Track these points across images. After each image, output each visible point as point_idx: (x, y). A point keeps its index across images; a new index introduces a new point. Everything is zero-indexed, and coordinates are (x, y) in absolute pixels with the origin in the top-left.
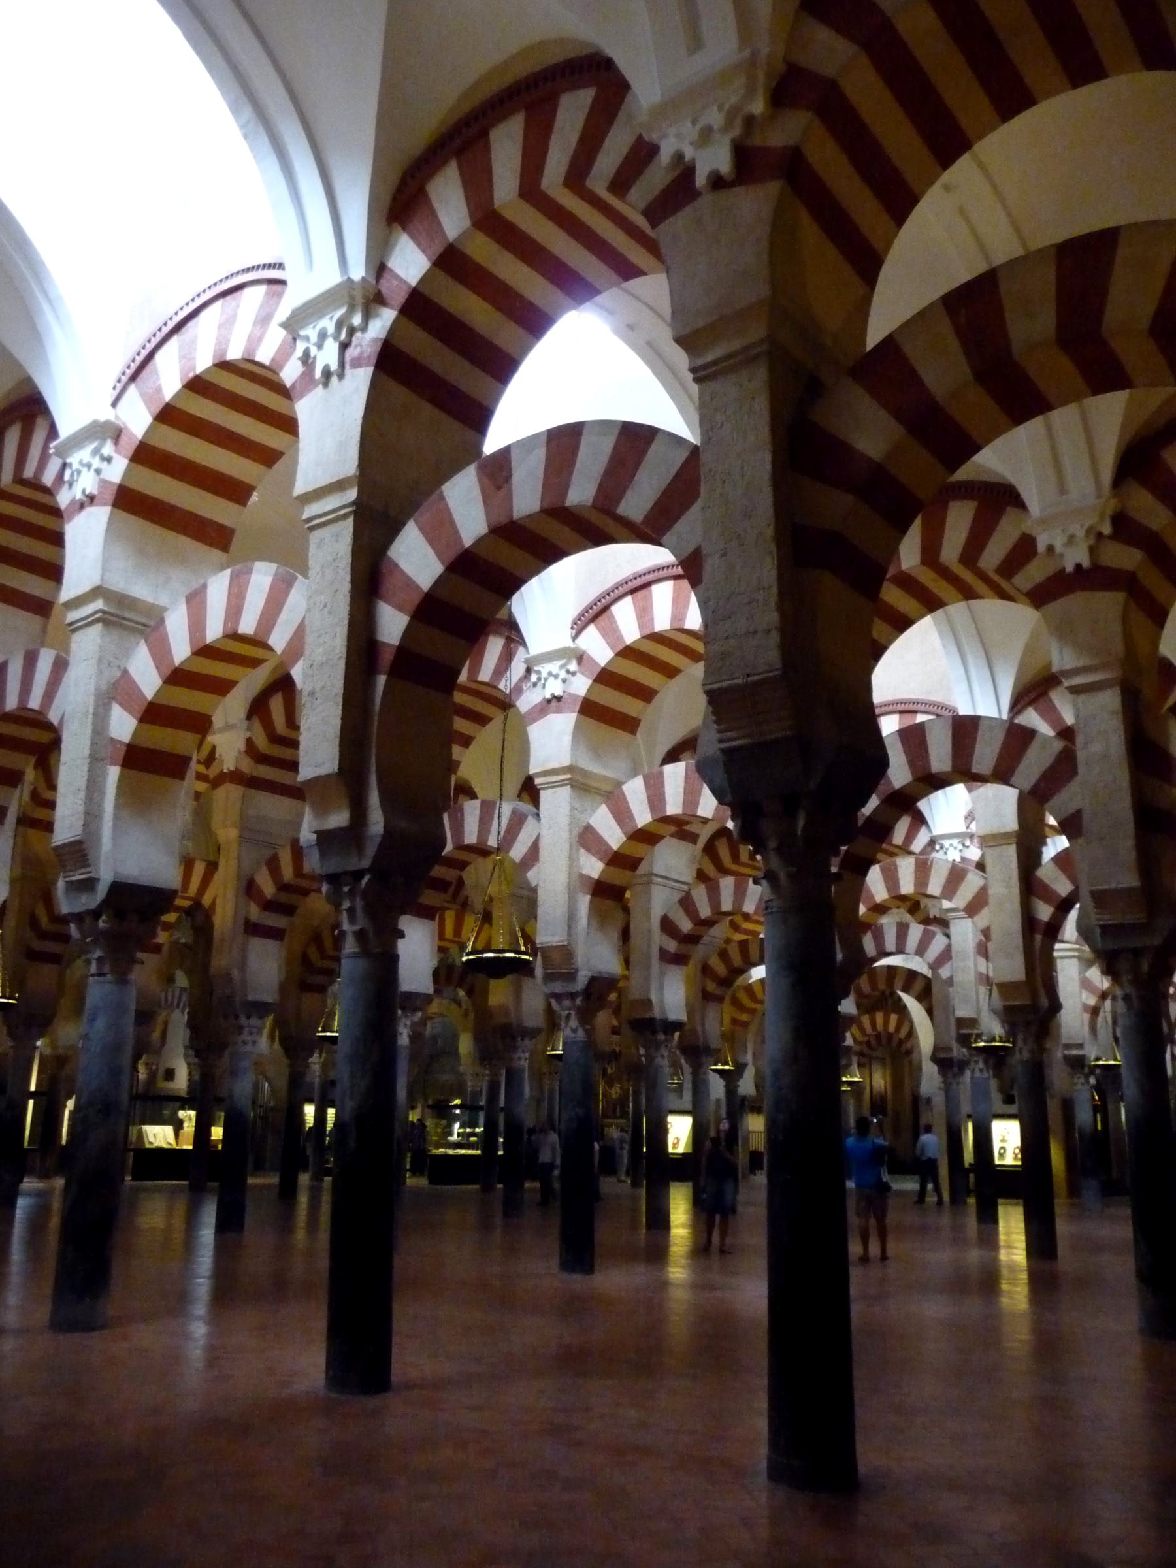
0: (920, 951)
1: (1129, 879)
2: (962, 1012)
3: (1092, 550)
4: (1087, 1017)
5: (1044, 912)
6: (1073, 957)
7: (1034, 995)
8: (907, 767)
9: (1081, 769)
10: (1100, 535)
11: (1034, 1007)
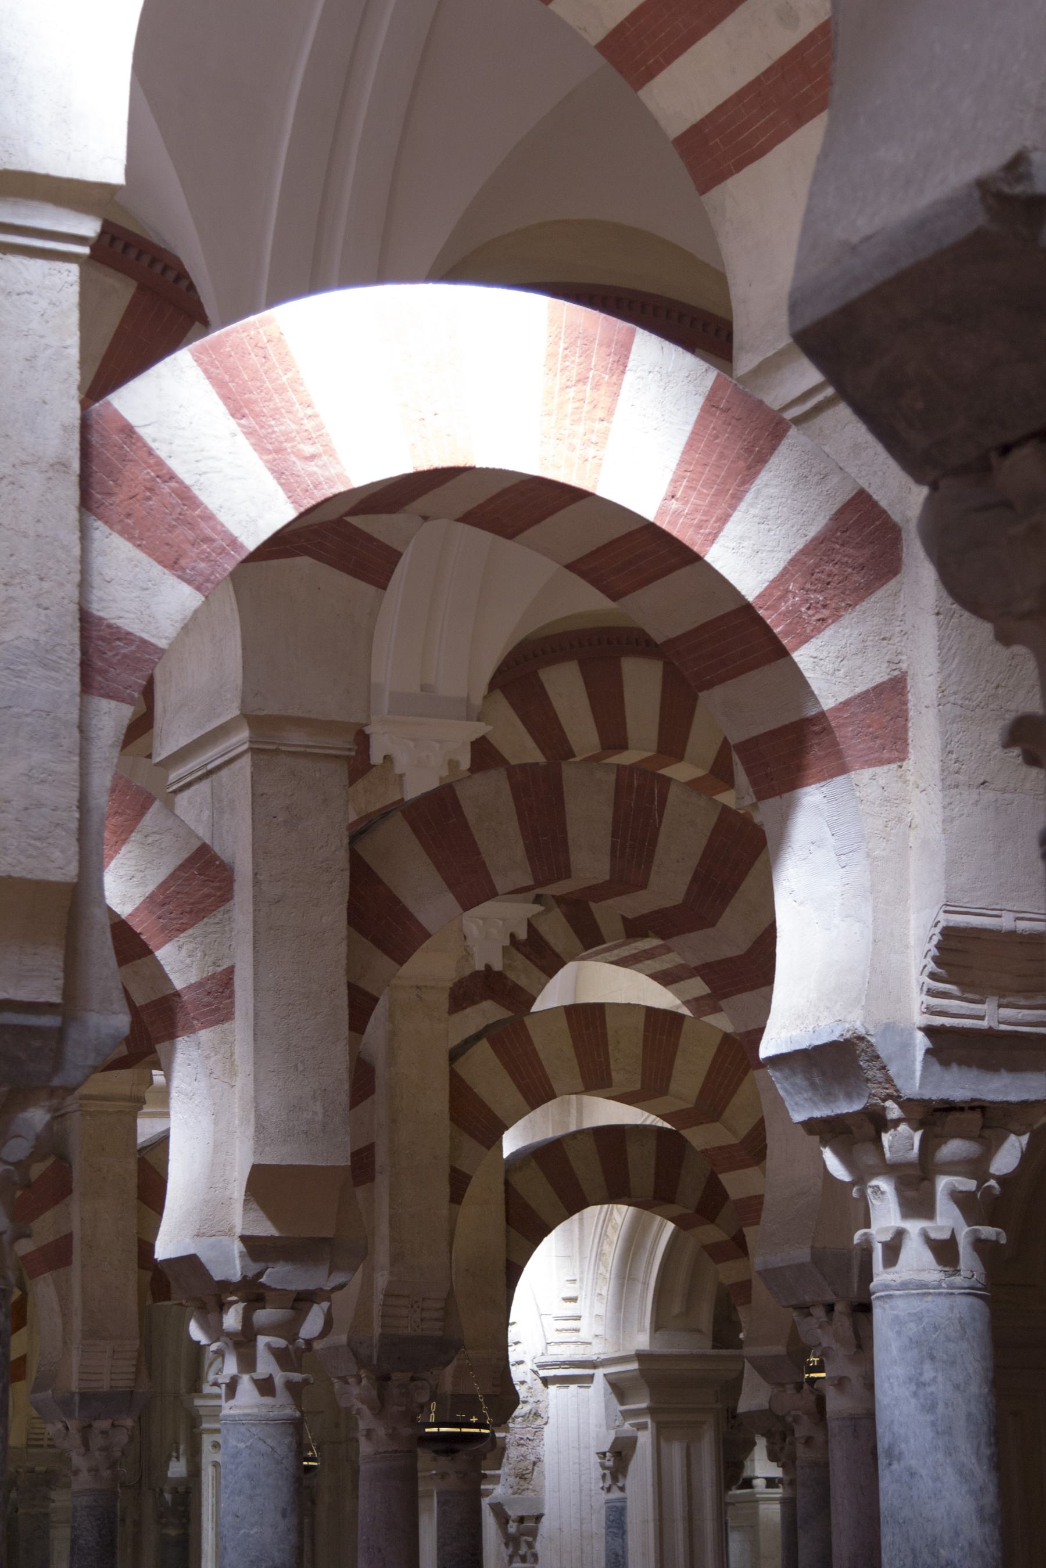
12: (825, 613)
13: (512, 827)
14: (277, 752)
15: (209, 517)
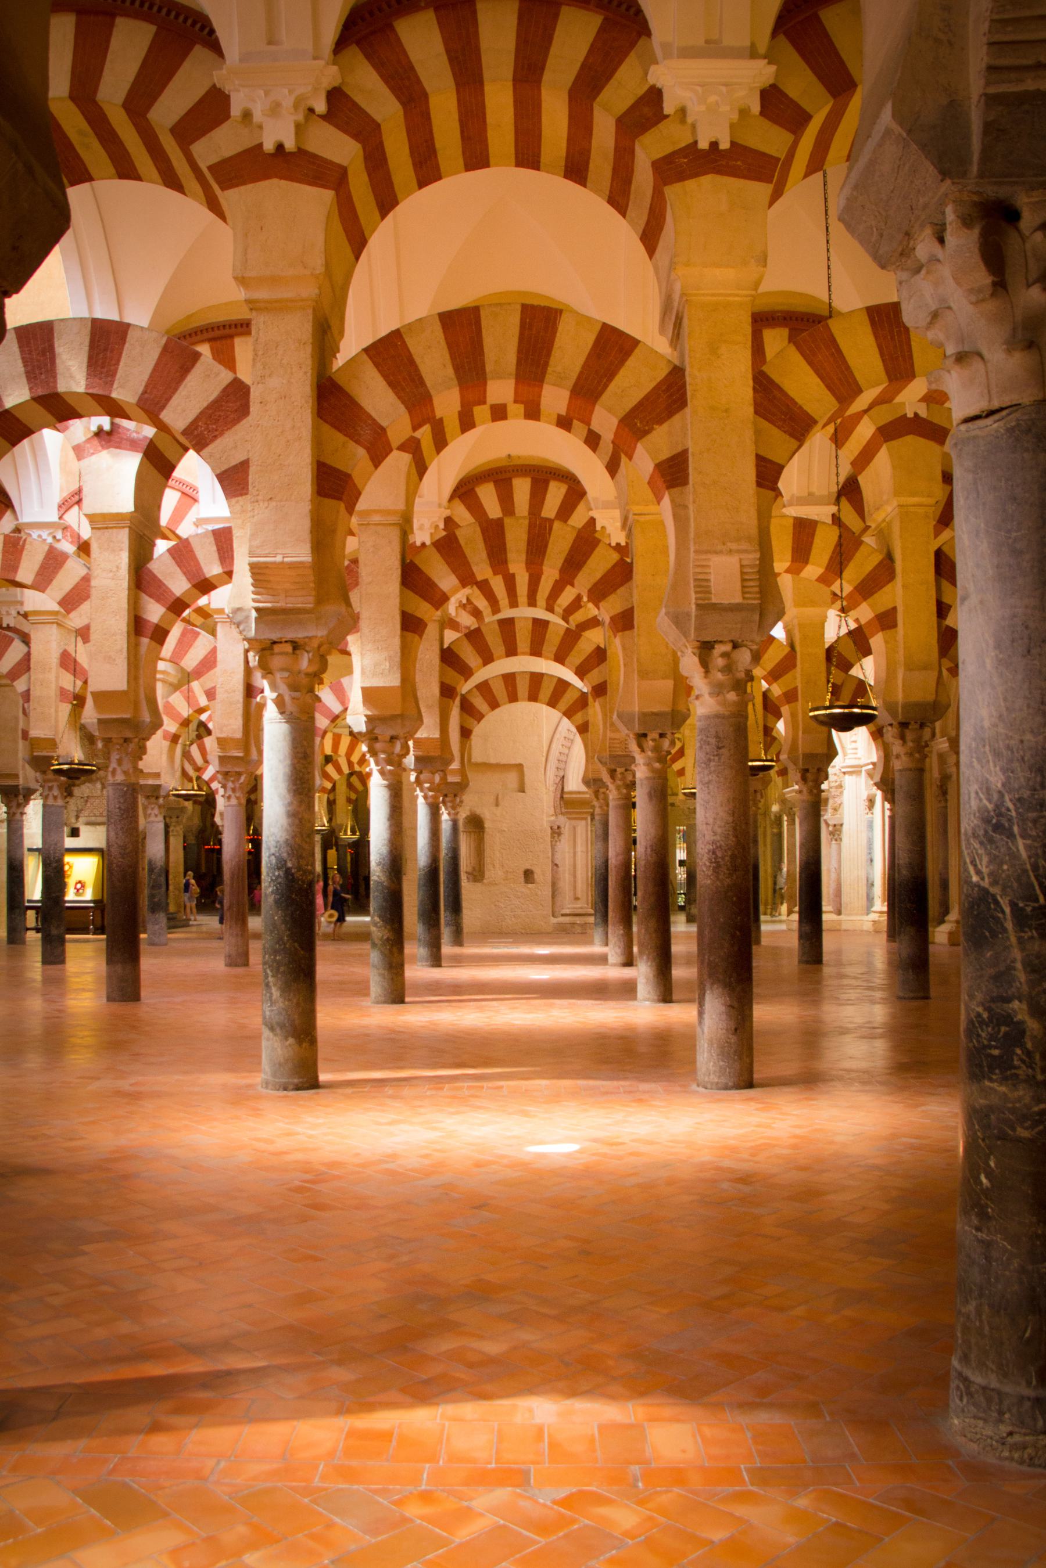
1: (302, 553)
9: (254, 407)
10: (311, 110)
12: (217, 433)
13: (481, 545)
14: (368, 524)
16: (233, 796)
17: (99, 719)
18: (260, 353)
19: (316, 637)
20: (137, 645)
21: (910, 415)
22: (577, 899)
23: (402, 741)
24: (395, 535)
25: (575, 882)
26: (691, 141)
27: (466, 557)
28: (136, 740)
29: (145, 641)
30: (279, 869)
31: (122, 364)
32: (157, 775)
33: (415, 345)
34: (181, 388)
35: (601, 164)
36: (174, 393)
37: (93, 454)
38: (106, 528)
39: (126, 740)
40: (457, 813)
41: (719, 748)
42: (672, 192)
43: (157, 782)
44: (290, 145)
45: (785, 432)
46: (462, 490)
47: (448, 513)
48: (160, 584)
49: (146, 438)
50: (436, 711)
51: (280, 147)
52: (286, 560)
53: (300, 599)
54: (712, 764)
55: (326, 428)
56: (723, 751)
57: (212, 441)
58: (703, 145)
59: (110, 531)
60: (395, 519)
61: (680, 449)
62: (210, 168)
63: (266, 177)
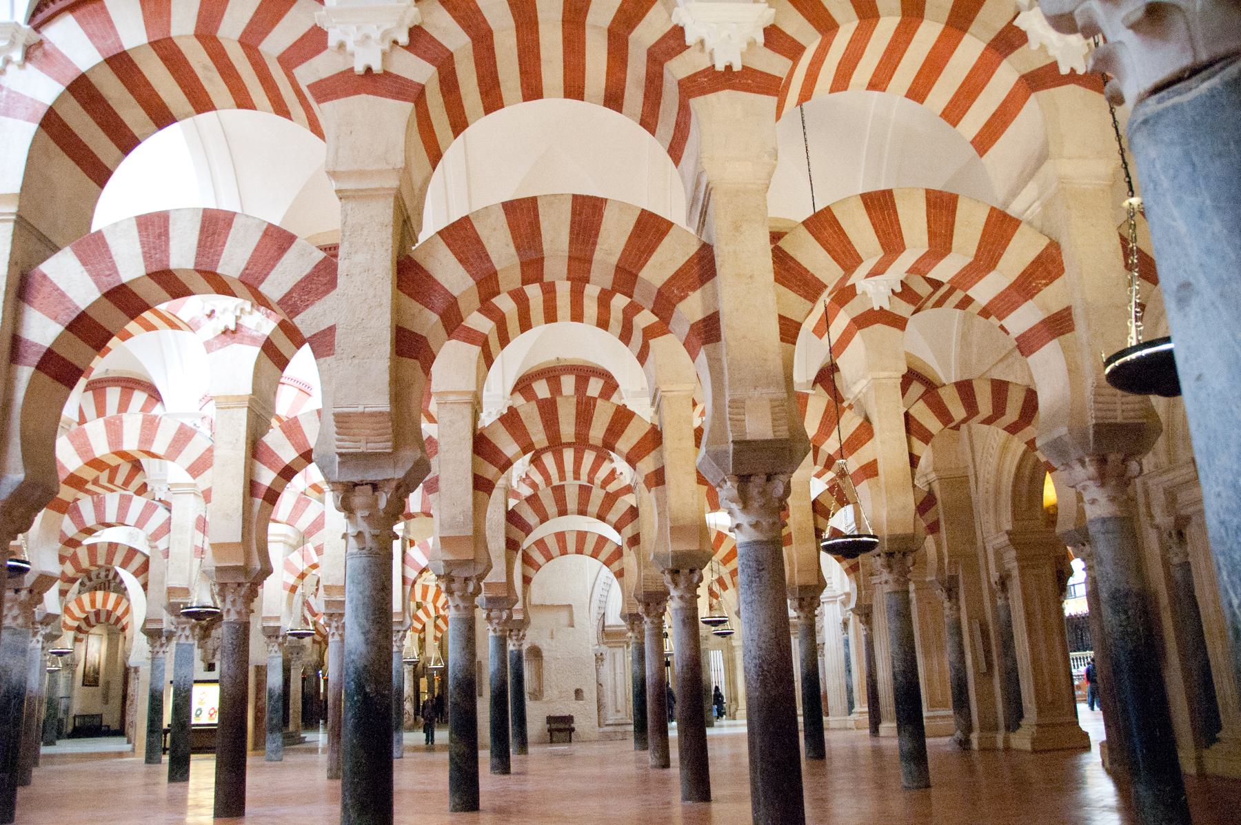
0: (140, 524)
1: (381, 403)
2: (176, 581)
3: (385, 55)
4: (286, 593)
5: (267, 477)
6: (281, 541)
7: (248, 555)
8: (141, 259)
9: (341, 280)
10: (395, 42)
11: (244, 570)
14: (446, 403)
15: (70, 301)
16: (336, 633)
17: (216, 567)
18: (348, 234)
19: (393, 479)
20: (251, 505)
21: (877, 308)
22: (618, 711)
23: (475, 581)
24: (468, 411)
25: (616, 698)
26: (709, 65)
27: (525, 429)
28: (248, 584)
29: (258, 501)
30: (359, 694)
31: (227, 245)
32: (278, 618)
33: (482, 230)
34: (278, 266)
35: (634, 94)
36: (271, 269)
37: (220, 348)
38: (229, 408)
39: (239, 585)
40: (521, 645)
41: (759, 570)
42: (696, 103)
43: (277, 624)
44: (377, 68)
45: (801, 295)
46: (520, 387)
47: (510, 403)
48: (272, 454)
49: (264, 335)
50: (503, 560)
51: (369, 70)
52: (367, 410)
53: (381, 445)
54: (754, 585)
55: (405, 299)
56: (763, 572)
57: (304, 310)
58: (720, 67)
59: (232, 410)
60: (468, 398)
61: (711, 312)
62: (309, 87)
63: (356, 92)
